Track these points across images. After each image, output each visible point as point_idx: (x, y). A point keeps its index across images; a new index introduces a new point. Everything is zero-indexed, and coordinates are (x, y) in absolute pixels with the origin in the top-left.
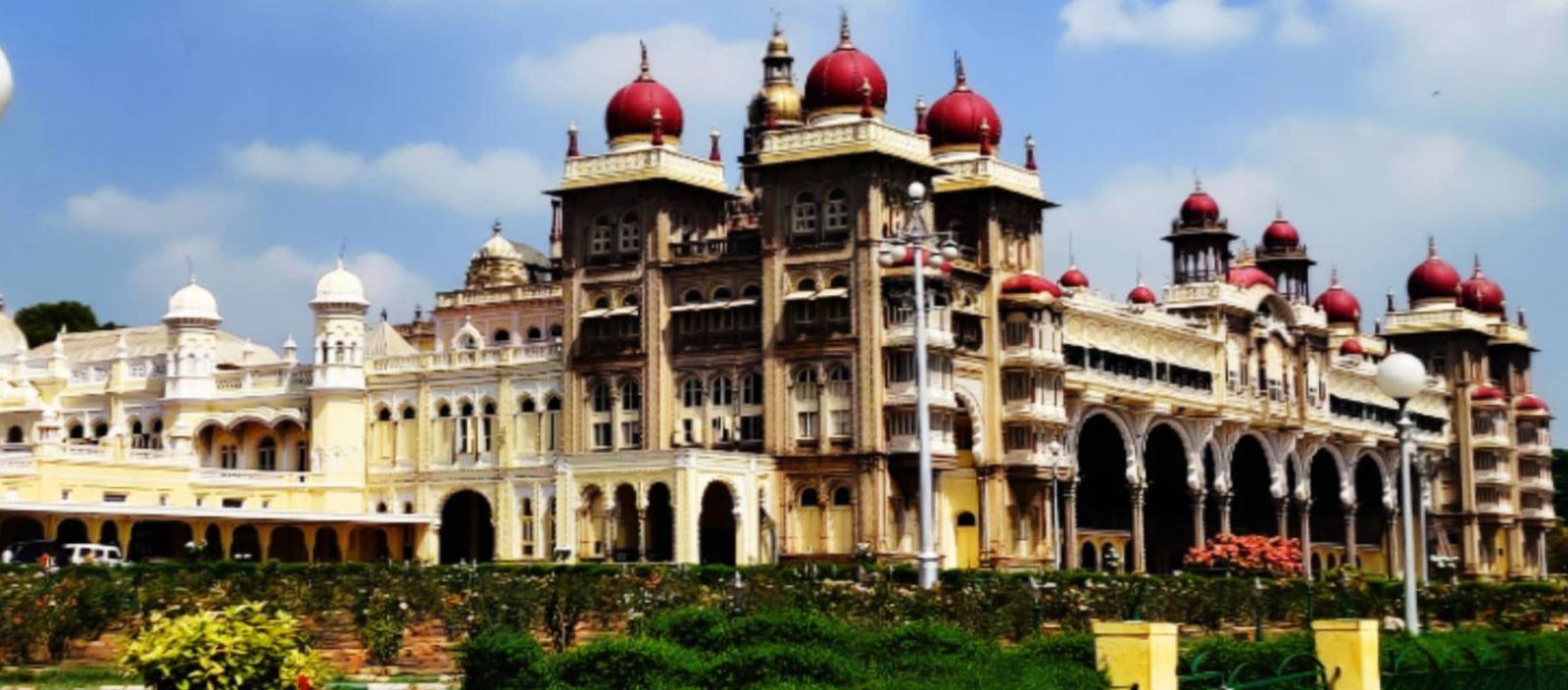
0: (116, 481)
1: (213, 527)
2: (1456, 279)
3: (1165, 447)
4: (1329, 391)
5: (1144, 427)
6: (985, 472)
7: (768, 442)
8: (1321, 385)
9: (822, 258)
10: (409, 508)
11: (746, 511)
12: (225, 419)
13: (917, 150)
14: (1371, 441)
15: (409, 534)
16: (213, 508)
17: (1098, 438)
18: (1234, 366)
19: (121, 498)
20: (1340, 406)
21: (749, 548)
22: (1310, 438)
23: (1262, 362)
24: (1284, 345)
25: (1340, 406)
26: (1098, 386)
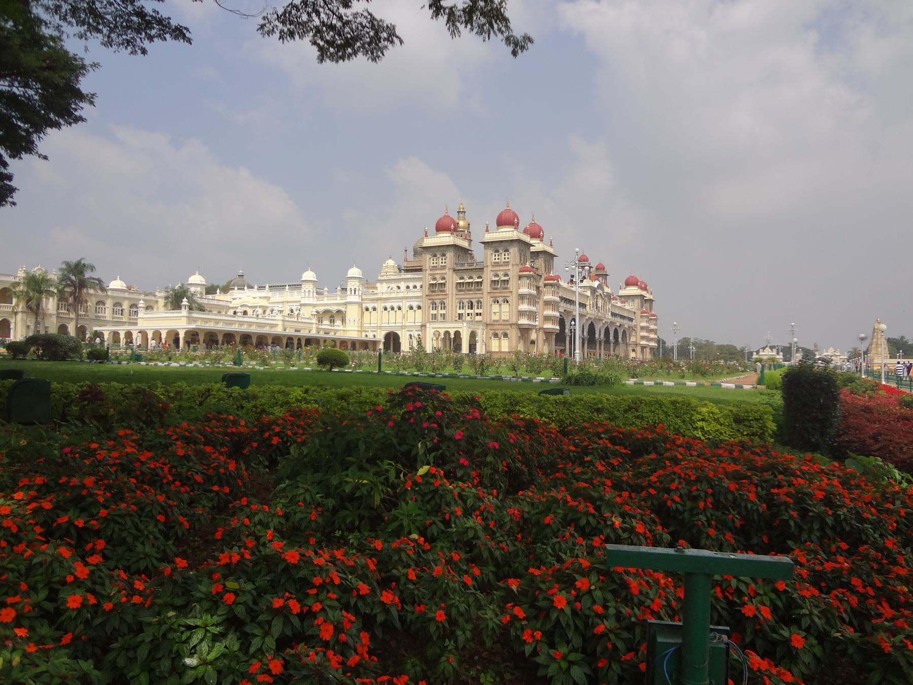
0: (298, 326)
2: (637, 281)
9: (502, 268)
15: (375, 343)
16: (322, 334)
19: (299, 331)
20: (614, 314)
21: (480, 350)
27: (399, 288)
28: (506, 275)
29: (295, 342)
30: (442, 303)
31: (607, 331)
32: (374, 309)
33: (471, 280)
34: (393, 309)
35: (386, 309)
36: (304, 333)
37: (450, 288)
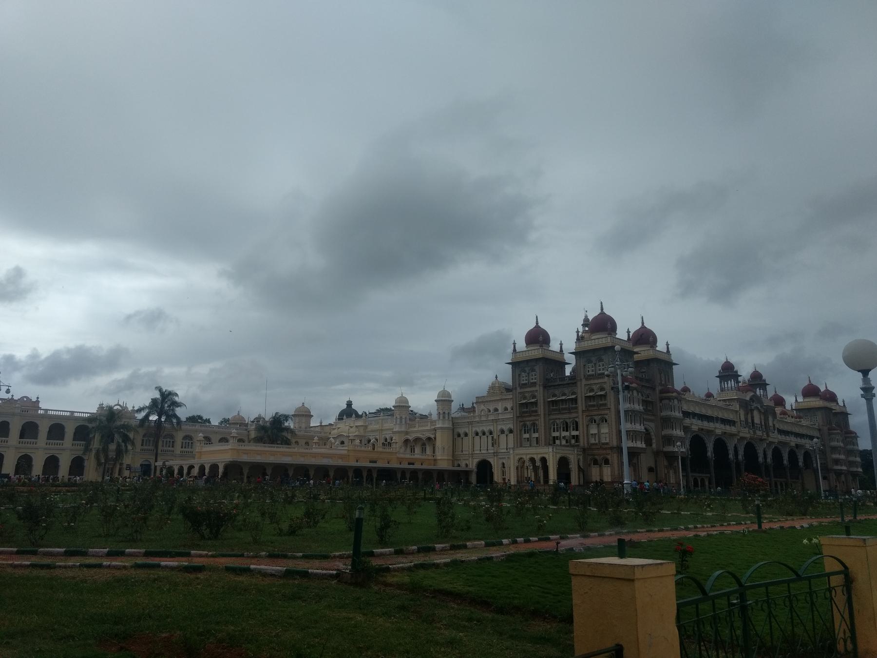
1: (403, 472)
3: (720, 444)
4: (777, 426)
5: (713, 439)
6: (657, 454)
7: (582, 443)
8: (774, 425)
9: (596, 381)
10: (467, 465)
11: (573, 467)
12: (411, 437)
13: (629, 346)
14: (793, 444)
15: (467, 473)
16: (405, 466)
17: (697, 442)
18: (743, 418)
19: (375, 462)
20: (780, 432)
21: (574, 480)
22: (771, 443)
23: (752, 418)
24: (760, 411)
25: (780, 432)
26: (696, 425)
27: (496, 410)
28: (602, 389)
29: (365, 474)
30: (534, 424)
31: (777, 453)
32: (466, 435)
33: (563, 398)
34: (484, 434)
35: (477, 434)
36: (380, 464)
37: (541, 409)
